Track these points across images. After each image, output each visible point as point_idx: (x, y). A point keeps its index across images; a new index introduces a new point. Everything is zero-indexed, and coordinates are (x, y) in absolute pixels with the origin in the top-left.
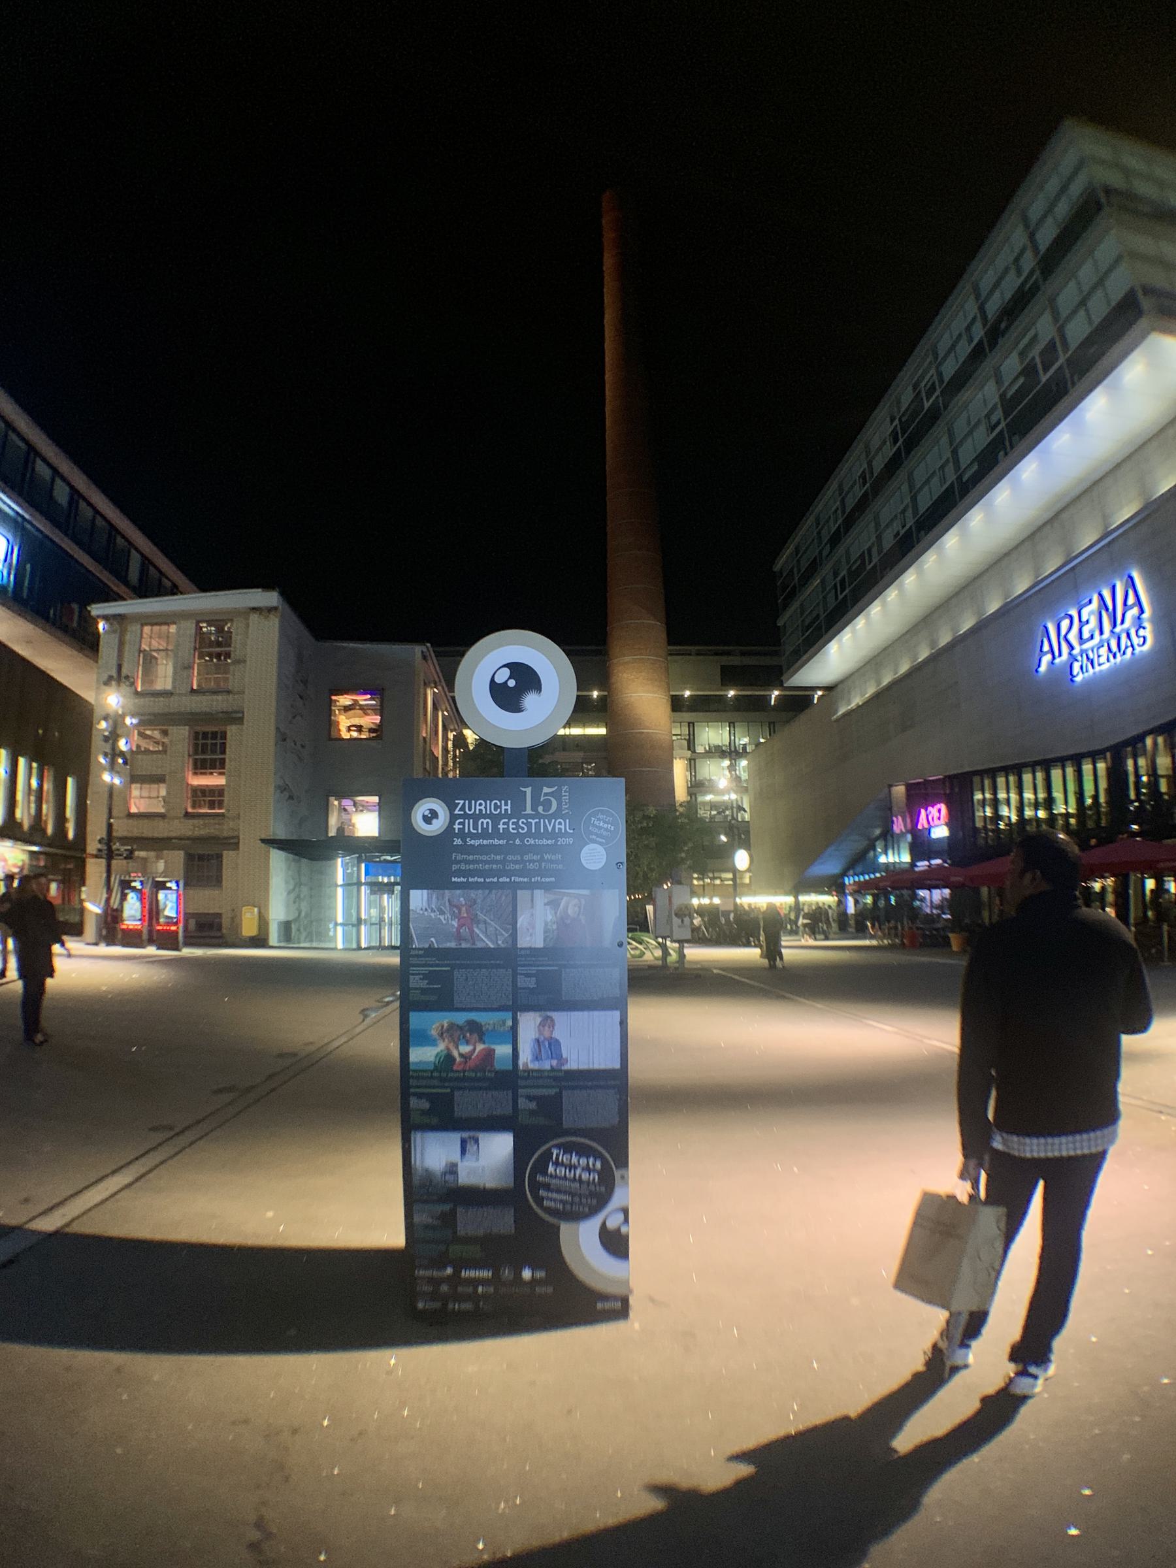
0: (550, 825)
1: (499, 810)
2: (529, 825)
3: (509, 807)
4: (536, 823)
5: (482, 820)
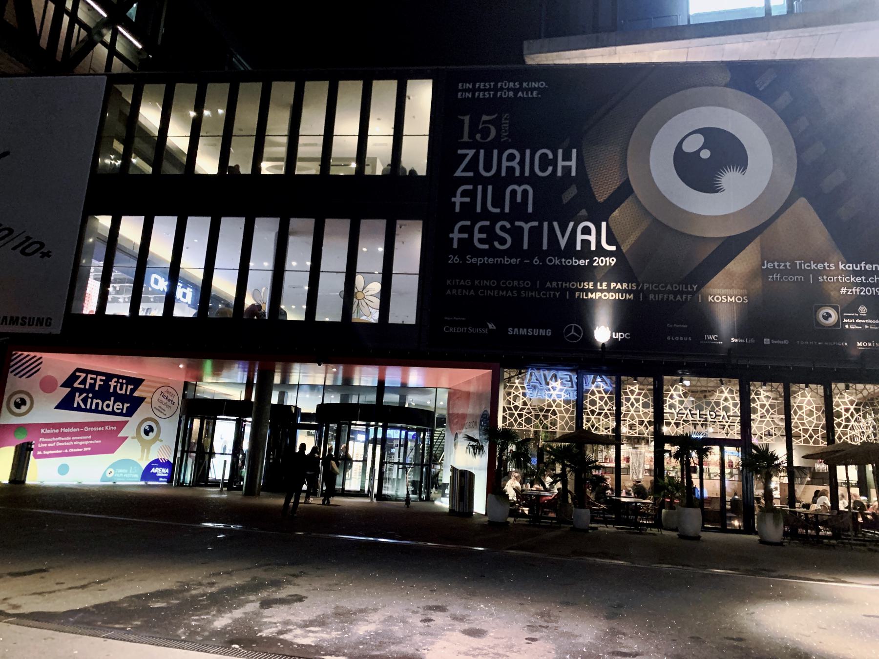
0: (563, 236)
1: (550, 169)
2: (517, 233)
3: (573, 163)
4: (531, 229)
5: (515, 187)
